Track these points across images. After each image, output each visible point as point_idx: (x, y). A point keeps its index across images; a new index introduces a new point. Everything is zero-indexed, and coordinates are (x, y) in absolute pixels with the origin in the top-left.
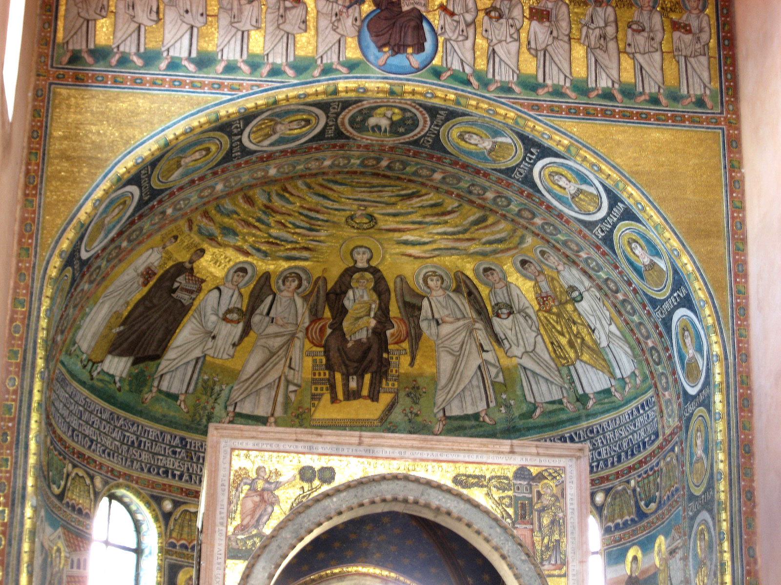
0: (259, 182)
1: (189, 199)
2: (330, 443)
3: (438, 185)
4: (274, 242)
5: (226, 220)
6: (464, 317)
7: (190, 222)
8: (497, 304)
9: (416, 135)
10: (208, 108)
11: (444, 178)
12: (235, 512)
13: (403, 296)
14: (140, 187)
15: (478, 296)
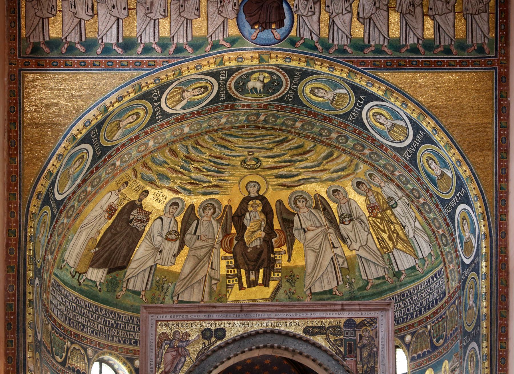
0: (178, 138)
4: (195, 183)
5: (160, 169)
6: (321, 226)
12: (160, 363)
13: (281, 214)
15: (330, 211)
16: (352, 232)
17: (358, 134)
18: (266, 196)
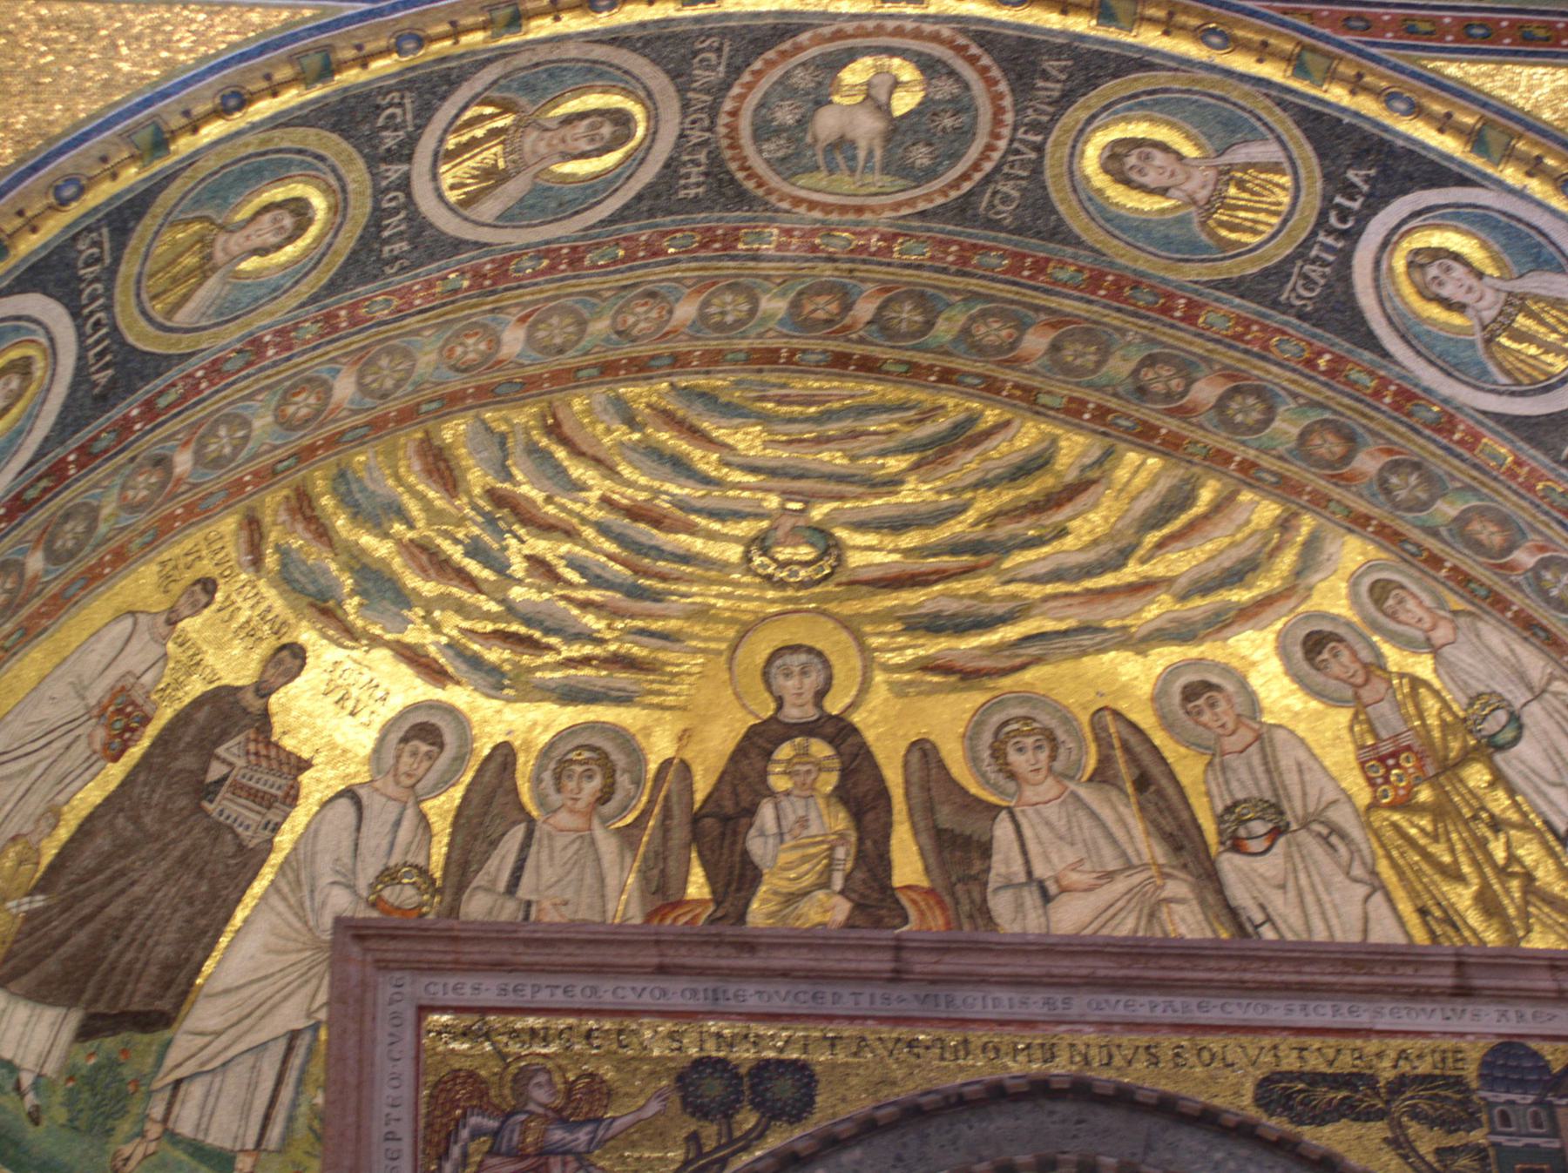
0: (470, 383)
1: (246, 424)
2: (785, 974)
3: (1036, 382)
5: (367, 540)
6: (1129, 866)
7: (253, 527)
8: (1229, 810)
9: (965, 177)
10: (295, 38)
11: (1055, 347)
13: (930, 810)
14: (76, 313)
15: (1170, 790)
16: (1283, 887)
17: (1331, 372)
18: (856, 718)
